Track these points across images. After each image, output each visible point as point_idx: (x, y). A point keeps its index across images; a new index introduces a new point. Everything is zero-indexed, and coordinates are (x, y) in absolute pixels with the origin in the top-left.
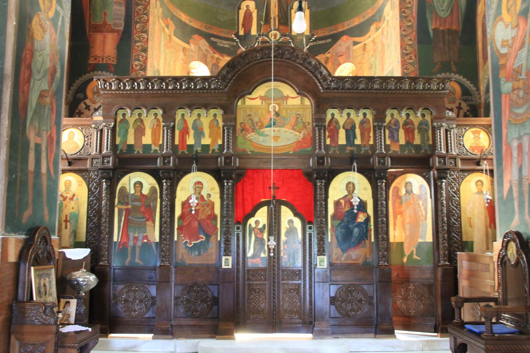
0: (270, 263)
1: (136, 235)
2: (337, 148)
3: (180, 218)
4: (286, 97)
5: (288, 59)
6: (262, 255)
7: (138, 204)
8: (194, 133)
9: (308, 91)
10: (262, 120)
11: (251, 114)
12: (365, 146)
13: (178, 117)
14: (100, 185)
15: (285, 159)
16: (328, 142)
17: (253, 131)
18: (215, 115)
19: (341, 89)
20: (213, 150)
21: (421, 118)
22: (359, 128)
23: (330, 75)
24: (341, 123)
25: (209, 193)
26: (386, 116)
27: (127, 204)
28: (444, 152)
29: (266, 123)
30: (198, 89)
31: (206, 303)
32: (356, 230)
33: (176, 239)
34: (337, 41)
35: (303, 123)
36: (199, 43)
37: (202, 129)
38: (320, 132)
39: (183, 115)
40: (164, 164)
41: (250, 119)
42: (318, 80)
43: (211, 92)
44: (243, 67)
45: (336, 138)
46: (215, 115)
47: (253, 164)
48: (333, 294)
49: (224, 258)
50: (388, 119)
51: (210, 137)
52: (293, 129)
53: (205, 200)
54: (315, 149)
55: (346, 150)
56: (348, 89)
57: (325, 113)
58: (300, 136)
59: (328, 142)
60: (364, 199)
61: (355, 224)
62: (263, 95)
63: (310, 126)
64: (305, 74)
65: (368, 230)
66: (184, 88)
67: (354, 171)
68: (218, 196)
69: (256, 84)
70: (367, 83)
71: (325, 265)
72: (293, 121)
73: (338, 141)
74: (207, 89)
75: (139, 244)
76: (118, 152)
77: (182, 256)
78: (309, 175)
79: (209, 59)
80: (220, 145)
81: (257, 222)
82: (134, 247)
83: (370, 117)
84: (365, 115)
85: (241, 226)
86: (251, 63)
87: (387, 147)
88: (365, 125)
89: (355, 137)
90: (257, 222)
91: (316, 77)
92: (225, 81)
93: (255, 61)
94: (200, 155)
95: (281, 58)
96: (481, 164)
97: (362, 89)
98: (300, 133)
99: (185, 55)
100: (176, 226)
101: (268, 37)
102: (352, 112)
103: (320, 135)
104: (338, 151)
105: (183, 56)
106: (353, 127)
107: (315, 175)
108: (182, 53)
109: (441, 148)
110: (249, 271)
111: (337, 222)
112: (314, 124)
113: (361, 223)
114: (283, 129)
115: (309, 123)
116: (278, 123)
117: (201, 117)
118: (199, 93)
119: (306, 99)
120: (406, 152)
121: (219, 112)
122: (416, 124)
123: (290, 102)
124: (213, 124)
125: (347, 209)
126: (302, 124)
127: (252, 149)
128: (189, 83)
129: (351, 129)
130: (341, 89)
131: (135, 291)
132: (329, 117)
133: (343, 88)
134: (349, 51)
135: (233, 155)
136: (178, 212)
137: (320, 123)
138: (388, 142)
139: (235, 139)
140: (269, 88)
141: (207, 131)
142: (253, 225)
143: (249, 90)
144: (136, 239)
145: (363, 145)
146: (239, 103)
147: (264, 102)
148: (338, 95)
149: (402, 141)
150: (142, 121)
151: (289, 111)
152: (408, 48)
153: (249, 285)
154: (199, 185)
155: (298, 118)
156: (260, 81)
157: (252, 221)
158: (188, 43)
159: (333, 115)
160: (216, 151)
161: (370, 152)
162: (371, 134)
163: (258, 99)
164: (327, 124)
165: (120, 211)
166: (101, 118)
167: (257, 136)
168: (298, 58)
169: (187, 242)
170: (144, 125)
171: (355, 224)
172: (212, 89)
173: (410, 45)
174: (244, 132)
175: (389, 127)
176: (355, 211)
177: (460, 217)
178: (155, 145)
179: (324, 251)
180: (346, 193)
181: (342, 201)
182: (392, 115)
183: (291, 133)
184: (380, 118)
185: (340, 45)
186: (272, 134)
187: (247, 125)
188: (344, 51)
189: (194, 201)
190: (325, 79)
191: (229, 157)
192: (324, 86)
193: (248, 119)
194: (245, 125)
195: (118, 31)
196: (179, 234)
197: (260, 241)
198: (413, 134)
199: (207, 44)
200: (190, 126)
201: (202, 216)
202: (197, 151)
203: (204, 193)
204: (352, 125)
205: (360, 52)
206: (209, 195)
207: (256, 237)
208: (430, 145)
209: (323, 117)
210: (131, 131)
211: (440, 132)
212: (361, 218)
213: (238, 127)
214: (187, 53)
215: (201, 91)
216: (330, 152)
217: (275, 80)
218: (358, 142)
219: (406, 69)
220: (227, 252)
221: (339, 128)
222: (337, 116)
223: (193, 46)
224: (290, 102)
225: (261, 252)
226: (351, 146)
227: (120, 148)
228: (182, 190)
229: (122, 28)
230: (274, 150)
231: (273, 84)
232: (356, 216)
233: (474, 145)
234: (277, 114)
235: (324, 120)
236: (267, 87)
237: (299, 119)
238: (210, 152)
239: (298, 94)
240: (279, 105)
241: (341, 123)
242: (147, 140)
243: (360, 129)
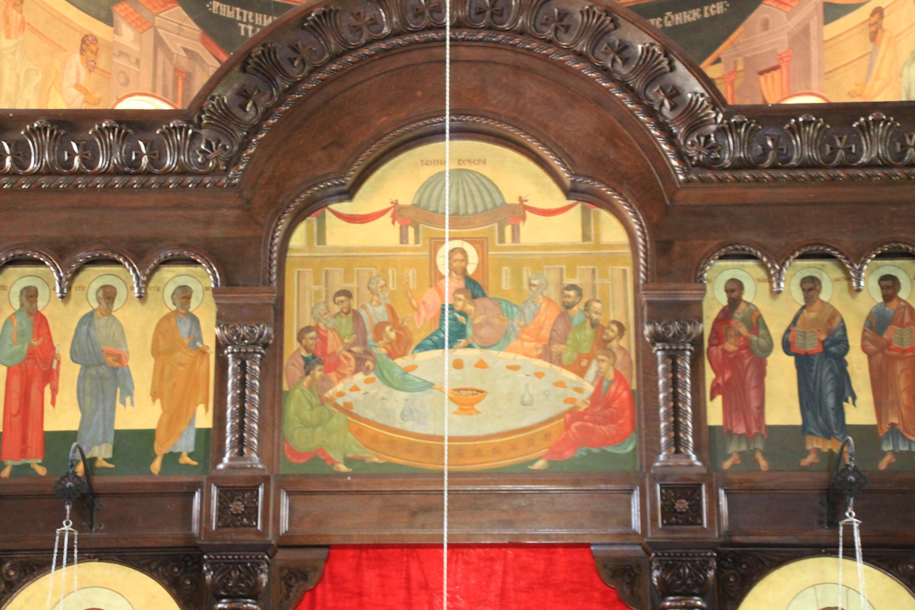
2: (760, 445)
4: (511, 207)
5: (522, 33)
8: (81, 378)
9: (618, 180)
11: (352, 286)
15: (511, 494)
16: (715, 413)
17: (360, 365)
18: (184, 294)
19: (774, 167)
20: (172, 458)
22: (864, 349)
23: (717, 101)
24: (777, 328)
29: (420, 329)
30: (104, 173)
34: (751, 10)
35: (594, 325)
36: (158, 21)
37: (120, 358)
38: (674, 369)
41: (349, 311)
42: (663, 126)
43: (163, 187)
44: (315, 70)
45: (753, 394)
46: (184, 294)
47: (355, 524)
51: (155, 395)
52: (547, 355)
54: (652, 449)
55: (807, 453)
56: (805, 165)
58: (579, 390)
59: (715, 413)
62: (406, 200)
63: (628, 342)
64: (601, 101)
66: (33, 166)
67: (850, 553)
69: (376, 149)
70: (899, 137)
72: (548, 316)
73: (761, 407)
74: (148, 173)
78: (625, 572)
80: (202, 434)
86: (350, 51)
88: (891, 334)
89: (844, 390)
91: (651, 112)
92: (230, 137)
93: (369, 43)
94: (107, 479)
95: (489, 28)
97: (871, 165)
99: (91, 68)
102: (828, 274)
103: (674, 383)
104: (765, 455)
105: (83, 72)
106: (836, 344)
107: (656, 573)
108: (76, 58)
112: (647, 330)
114: (499, 358)
115: (621, 328)
116: (475, 327)
117: (117, 304)
118: (108, 188)
119: (605, 216)
121: (200, 279)
123: (535, 231)
126: (589, 332)
127: (356, 449)
128: (60, 143)
129: (826, 352)
130: (774, 167)
132: (715, 300)
133: (782, 163)
134: (807, 49)
135: (266, 480)
137: (675, 328)
139: (274, 400)
140: (437, 169)
141: (141, 370)
143: (341, 175)
145: (885, 428)
146: (298, 239)
147: (411, 230)
148: (756, 194)
155: (569, 307)
156: (388, 141)
158: (109, 20)
159: (734, 288)
160: (185, 459)
163: (387, 218)
164: (706, 327)
167: (379, 389)
168: (567, 29)
172: (169, 173)
174: (318, 372)
183: (540, 375)
185: (766, 25)
186: (448, 378)
187: (330, 336)
188: (782, 49)
190: (695, 123)
191: (243, 490)
192: (692, 152)
193: (336, 309)
194: (324, 339)
199: (192, 28)
200: (63, 346)
202: (90, 464)
204: (830, 334)
205: (858, 45)
213: (292, 346)
214: (102, 62)
215: (117, 181)
216: (727, 465)
217: (459, 133)
218: (860, 412)
221: (769, 349)
222: (754, 293)
223: (127, 35)
230: (458, 453)
231: (449, 152)
234: (474, 288)
235: (691, 311)
236: (427, 163)
238: (156, 466)
239: (570, 192)
240: (480, 244)
241: (777, 328)
243: (870, 356)
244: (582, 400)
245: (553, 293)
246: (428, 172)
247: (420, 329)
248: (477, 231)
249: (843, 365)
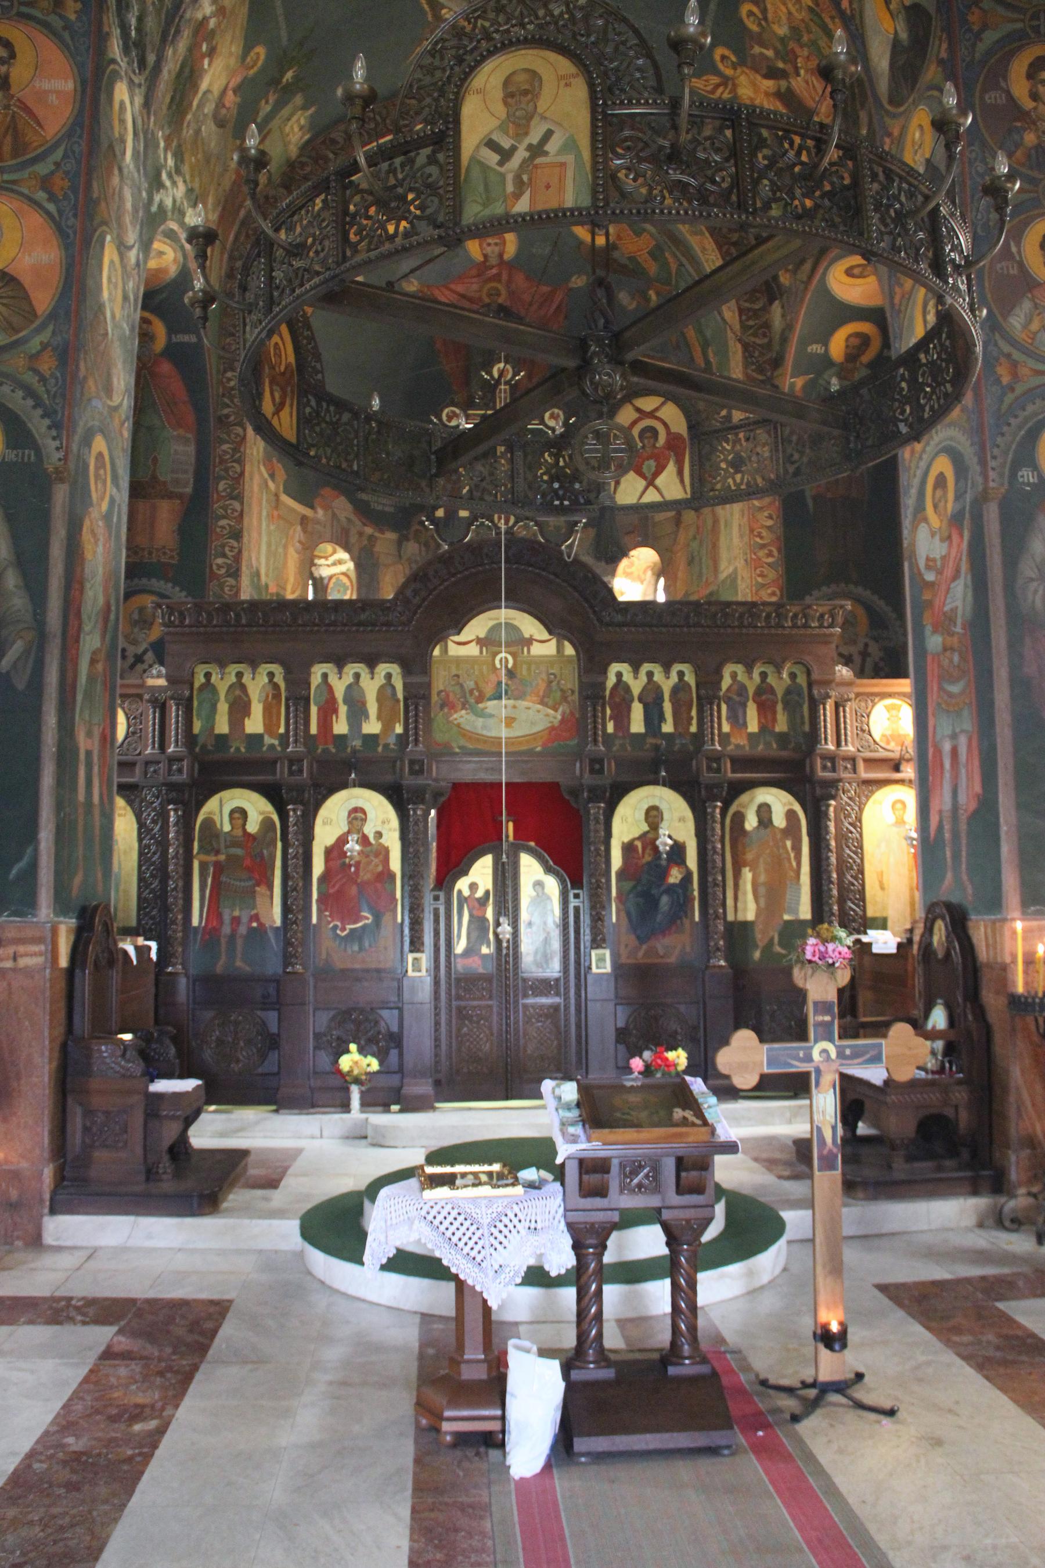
0: (499, 965)
1: (236, 913)
3: (322, 879)
6: (485, 950)
7: (239, 852)
10: (481, 685)
12: (681, 735)
13: (316, 680)
14: (164, 815)
16: (610, 728)
18: (389, 676)
20: (386, 746)
21: (789, 681)
25: (379, 829)
26: (721, 677)
27: (217, 852)
28: (831, 747)
29: (489, 690)
31: (377, 1043)
32: (665, 900)
33: (314, 920)
35: (562, 690)
38: (595, 710)
39: (325, 676)
40: (291, 773)
46: (389, 676)
48: (621, 1024)
49: (410, 957)
50: (726, 682)
51: (379, 718)
52: (542, 703)
53: (370, 844)
57: (604, 672)
59: (610, 728)
60: (680, 839)
61: (663, 888)
62: (482, 635)
65: (689, 900)
68: (396, 835)
71: (608, 968)
72: (542, 686)
75: (243, 930)
76: (197, 750)
77: (328, 954)
79: (353, 539)
80: (399, 736)
81: (473, 887)
82: (232, 937)
83: (690, 678)
84: (681, 674)
85: (442, 894)
87: (724, 738)
88: (682, 695)
89: (662, 718)
90: (473, 887)
96: (902, 768)
98: (556, 710)
100: (315, 896)
101: (492, 521)
106: (660, 699)
109: (826, 739)
110: (458, 980)
111: (628, 885)
113: (674, 885)
114: (523, 704)
120: (761, 747)
121: (395, 669)
122: (780, 694)
123: (537, 650)
124: (386, 692)
125: (648, 858)
131: (236, 1023)
132: (611, 680)
136: (318, 867)
138: (726, 728)
141: (372, 708)
142: (466, 893)
144: (236, 921)
146: (437, 652)
149: (753, 727)
150: (243, 688)
151: (533, 667)
152: (764, 533)
153: (459, 1010)
154: (357, 815)
157: (462, 885)
159: (619, 675)
161: (691, 748)
162: (694, 713)
163: (473, 644)
165: (203, 867)
166: (162, 682)
167: (472, 717)
169: (335, 927)
170: (247, 695)
171: (663, 888)
173: (769, 528)
174: (446, 710)
175: (728, 700)
176: (664, 863)
177: (861, 871)
178: (271, 736)
179: (604, 940)
180: (645, 828)
181: (639, 844)
182: (734, 676)
184: (709, 681)
189: (353, 846)
195: (180, 496)
196: (320, 911)
197: (479, 924)
198: (774, 713)
201: (365, 876)
203: (369, 830)
206: (379, 835)
207: (471, 915)
208: (804, 733)
209: (600, 679)
210: (223, 708)
211: (825, 709)
212: (675, 876)
213: (435, 698)
218: (668, 728)
219: (762, 575)
220: (416, 945)
221: (632, 700)
224: (537, 650)
225: (482, 944)
226: (654, 736)
227: (201, 740)
228: (324, 823)
229: (189, 490)
232: (665, 873)
233: (888, 733)
234: (511, 674)
237: (554, 684)
238: (380, 749)
242: (254, 724)
244: (556, 723)
245: (544, 676)
246: (491, 623)
247: (489, 690)
248: (512, 649)
249: (662, 708)
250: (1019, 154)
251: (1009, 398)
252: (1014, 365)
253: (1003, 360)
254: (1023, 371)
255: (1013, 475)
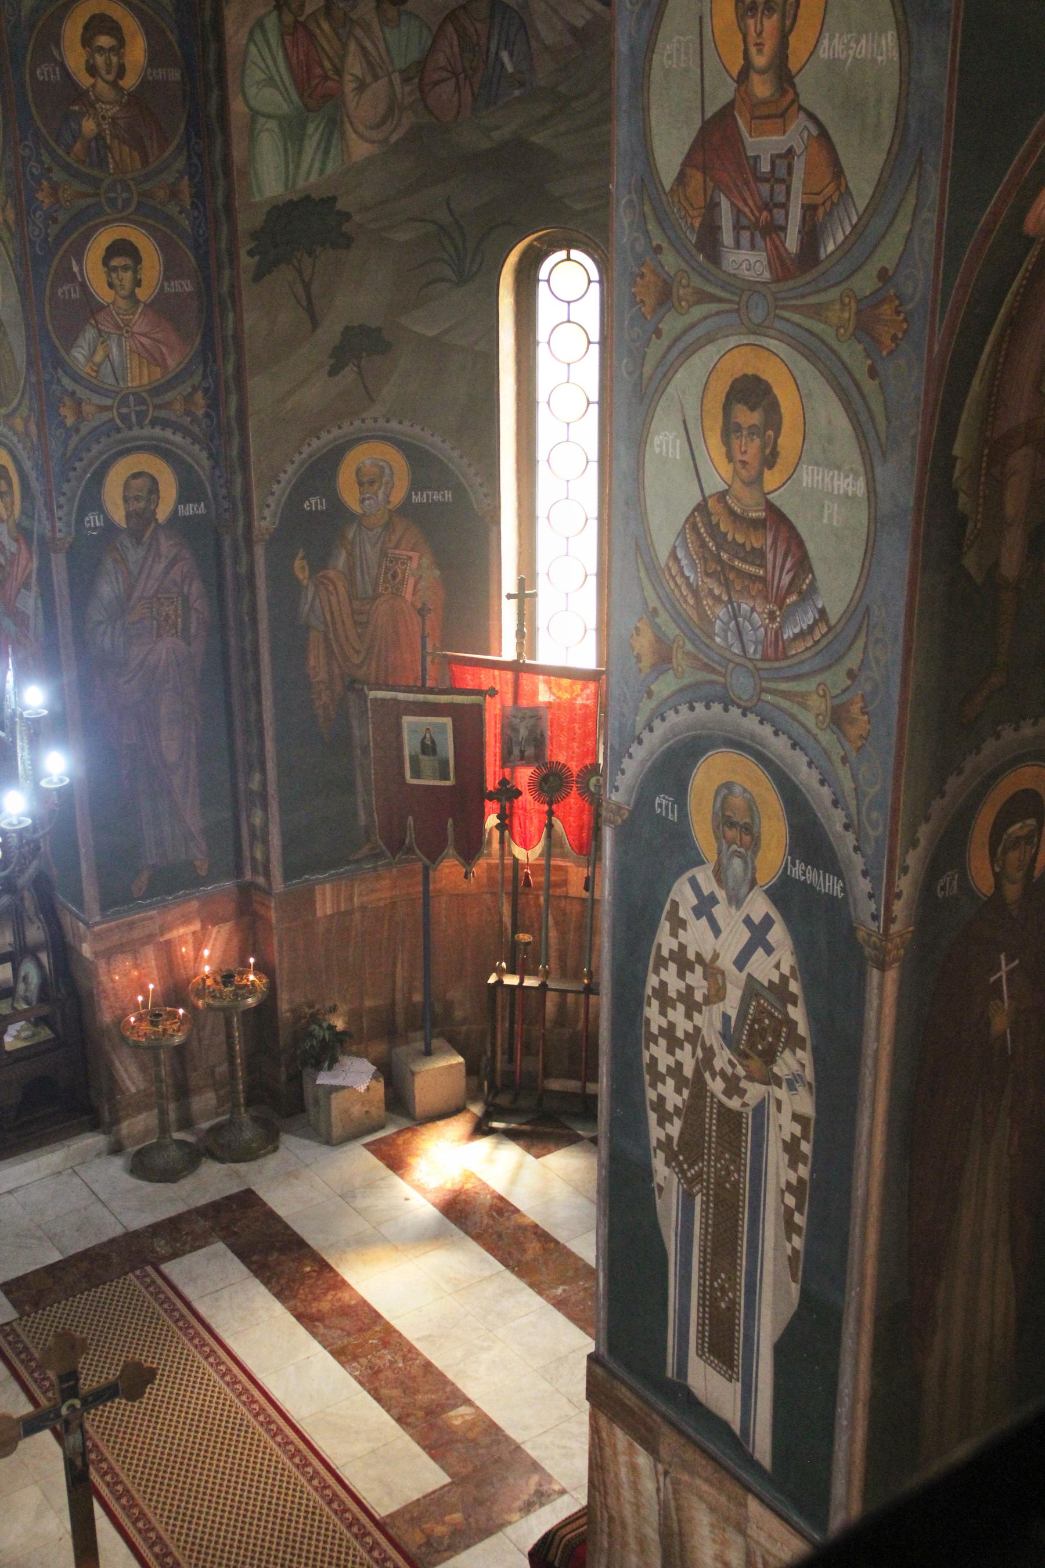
250: (78, 146)
251: (75, 439)
252: (79, 403)
253: (67, 400)
254: (87, 409)
255: (80, 521)
